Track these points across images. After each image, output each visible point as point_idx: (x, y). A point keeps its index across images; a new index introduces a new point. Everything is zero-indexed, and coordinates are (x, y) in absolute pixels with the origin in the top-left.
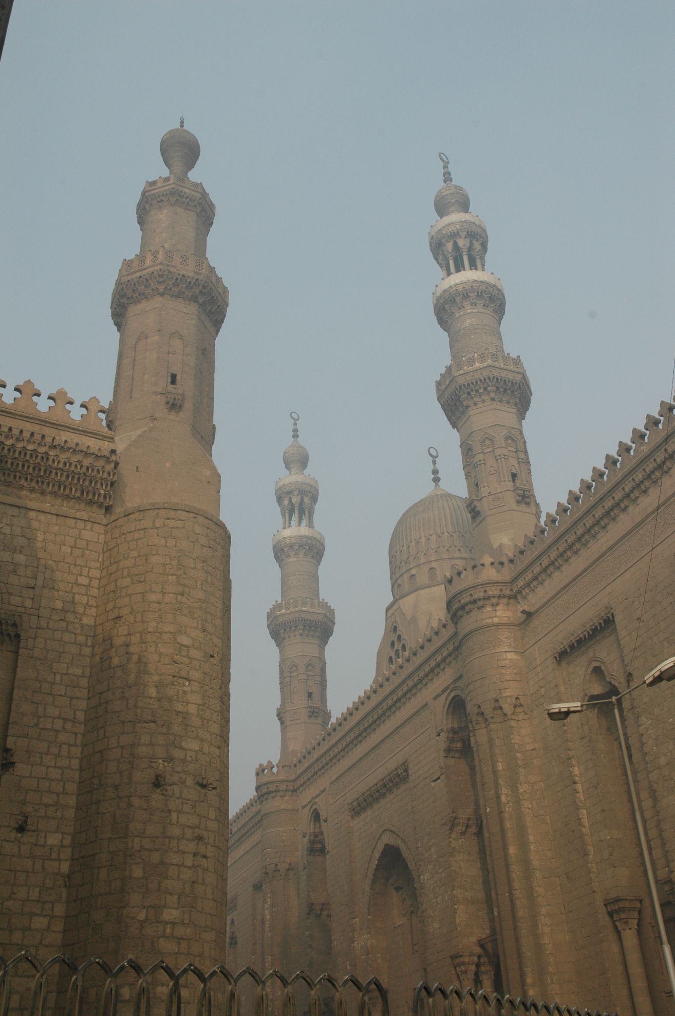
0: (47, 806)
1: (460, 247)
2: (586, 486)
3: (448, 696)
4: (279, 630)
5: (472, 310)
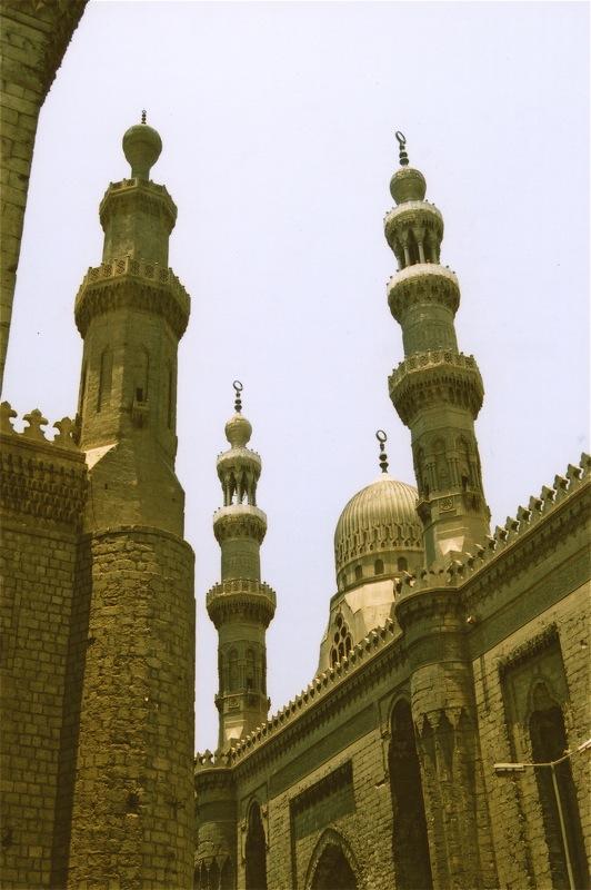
0: (29, 820)
1: (416, 236)
2: (536, 505)
3: (393, 699)
4: (218, 613)
5: (425, 305)
